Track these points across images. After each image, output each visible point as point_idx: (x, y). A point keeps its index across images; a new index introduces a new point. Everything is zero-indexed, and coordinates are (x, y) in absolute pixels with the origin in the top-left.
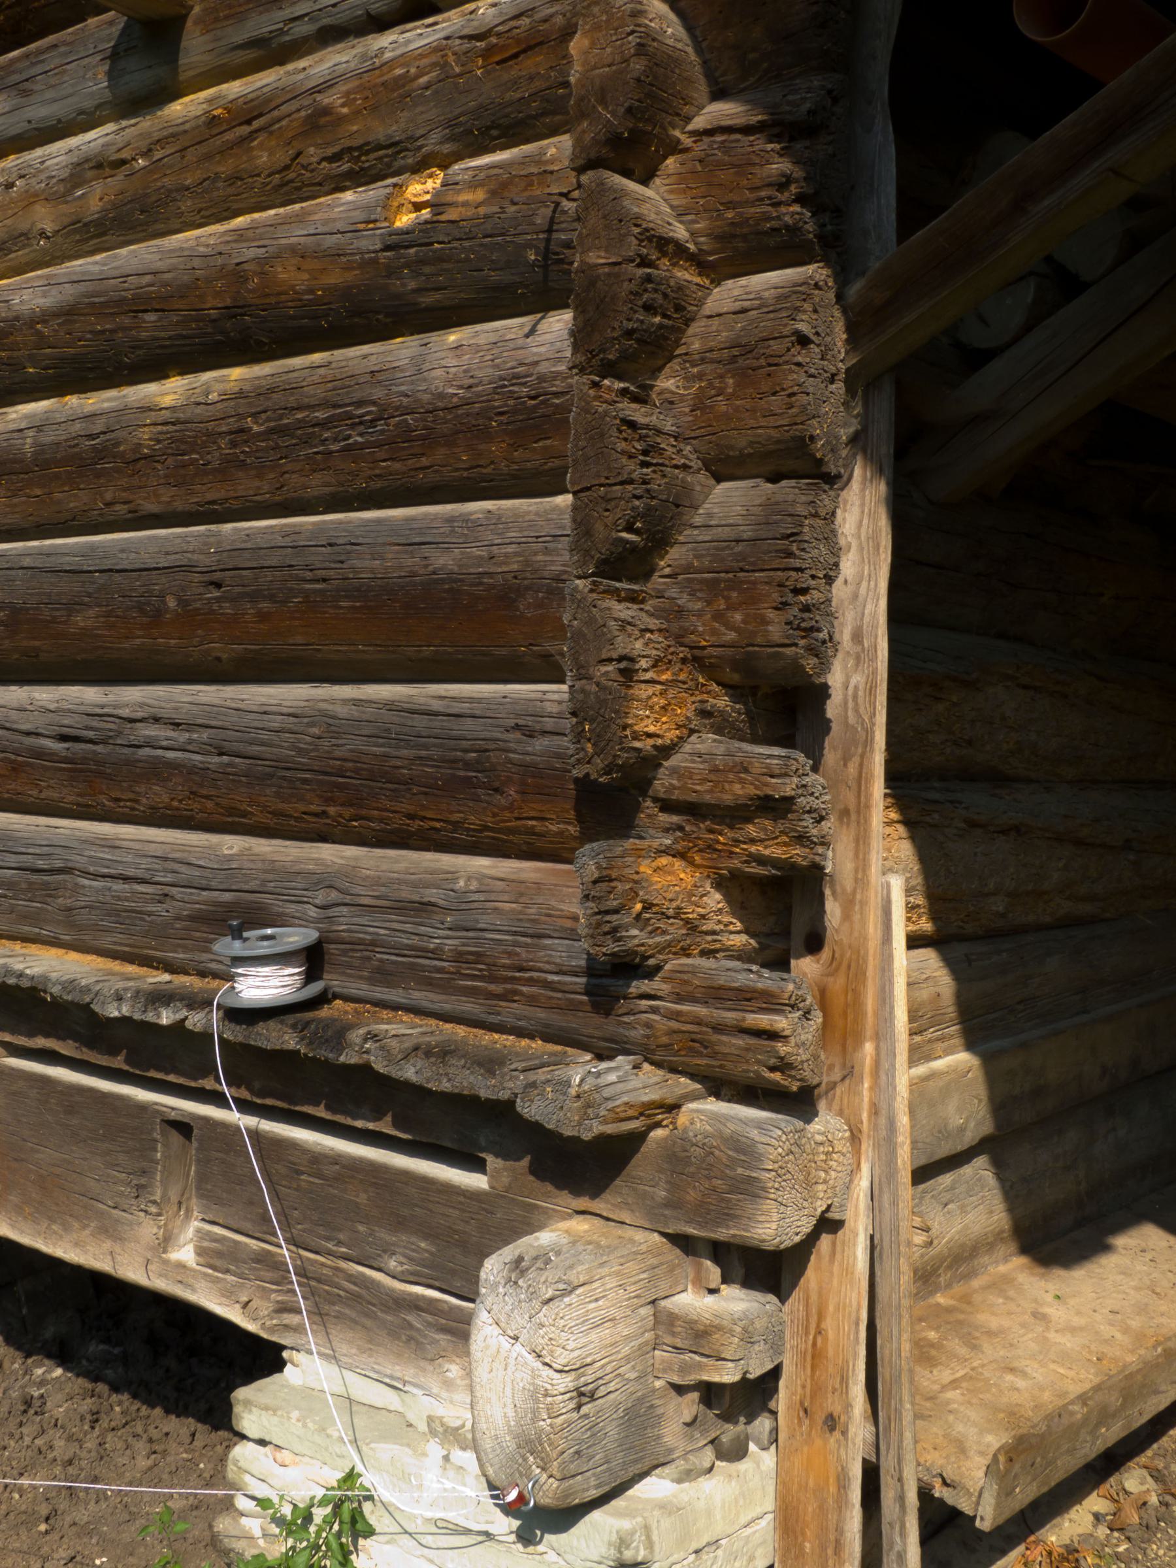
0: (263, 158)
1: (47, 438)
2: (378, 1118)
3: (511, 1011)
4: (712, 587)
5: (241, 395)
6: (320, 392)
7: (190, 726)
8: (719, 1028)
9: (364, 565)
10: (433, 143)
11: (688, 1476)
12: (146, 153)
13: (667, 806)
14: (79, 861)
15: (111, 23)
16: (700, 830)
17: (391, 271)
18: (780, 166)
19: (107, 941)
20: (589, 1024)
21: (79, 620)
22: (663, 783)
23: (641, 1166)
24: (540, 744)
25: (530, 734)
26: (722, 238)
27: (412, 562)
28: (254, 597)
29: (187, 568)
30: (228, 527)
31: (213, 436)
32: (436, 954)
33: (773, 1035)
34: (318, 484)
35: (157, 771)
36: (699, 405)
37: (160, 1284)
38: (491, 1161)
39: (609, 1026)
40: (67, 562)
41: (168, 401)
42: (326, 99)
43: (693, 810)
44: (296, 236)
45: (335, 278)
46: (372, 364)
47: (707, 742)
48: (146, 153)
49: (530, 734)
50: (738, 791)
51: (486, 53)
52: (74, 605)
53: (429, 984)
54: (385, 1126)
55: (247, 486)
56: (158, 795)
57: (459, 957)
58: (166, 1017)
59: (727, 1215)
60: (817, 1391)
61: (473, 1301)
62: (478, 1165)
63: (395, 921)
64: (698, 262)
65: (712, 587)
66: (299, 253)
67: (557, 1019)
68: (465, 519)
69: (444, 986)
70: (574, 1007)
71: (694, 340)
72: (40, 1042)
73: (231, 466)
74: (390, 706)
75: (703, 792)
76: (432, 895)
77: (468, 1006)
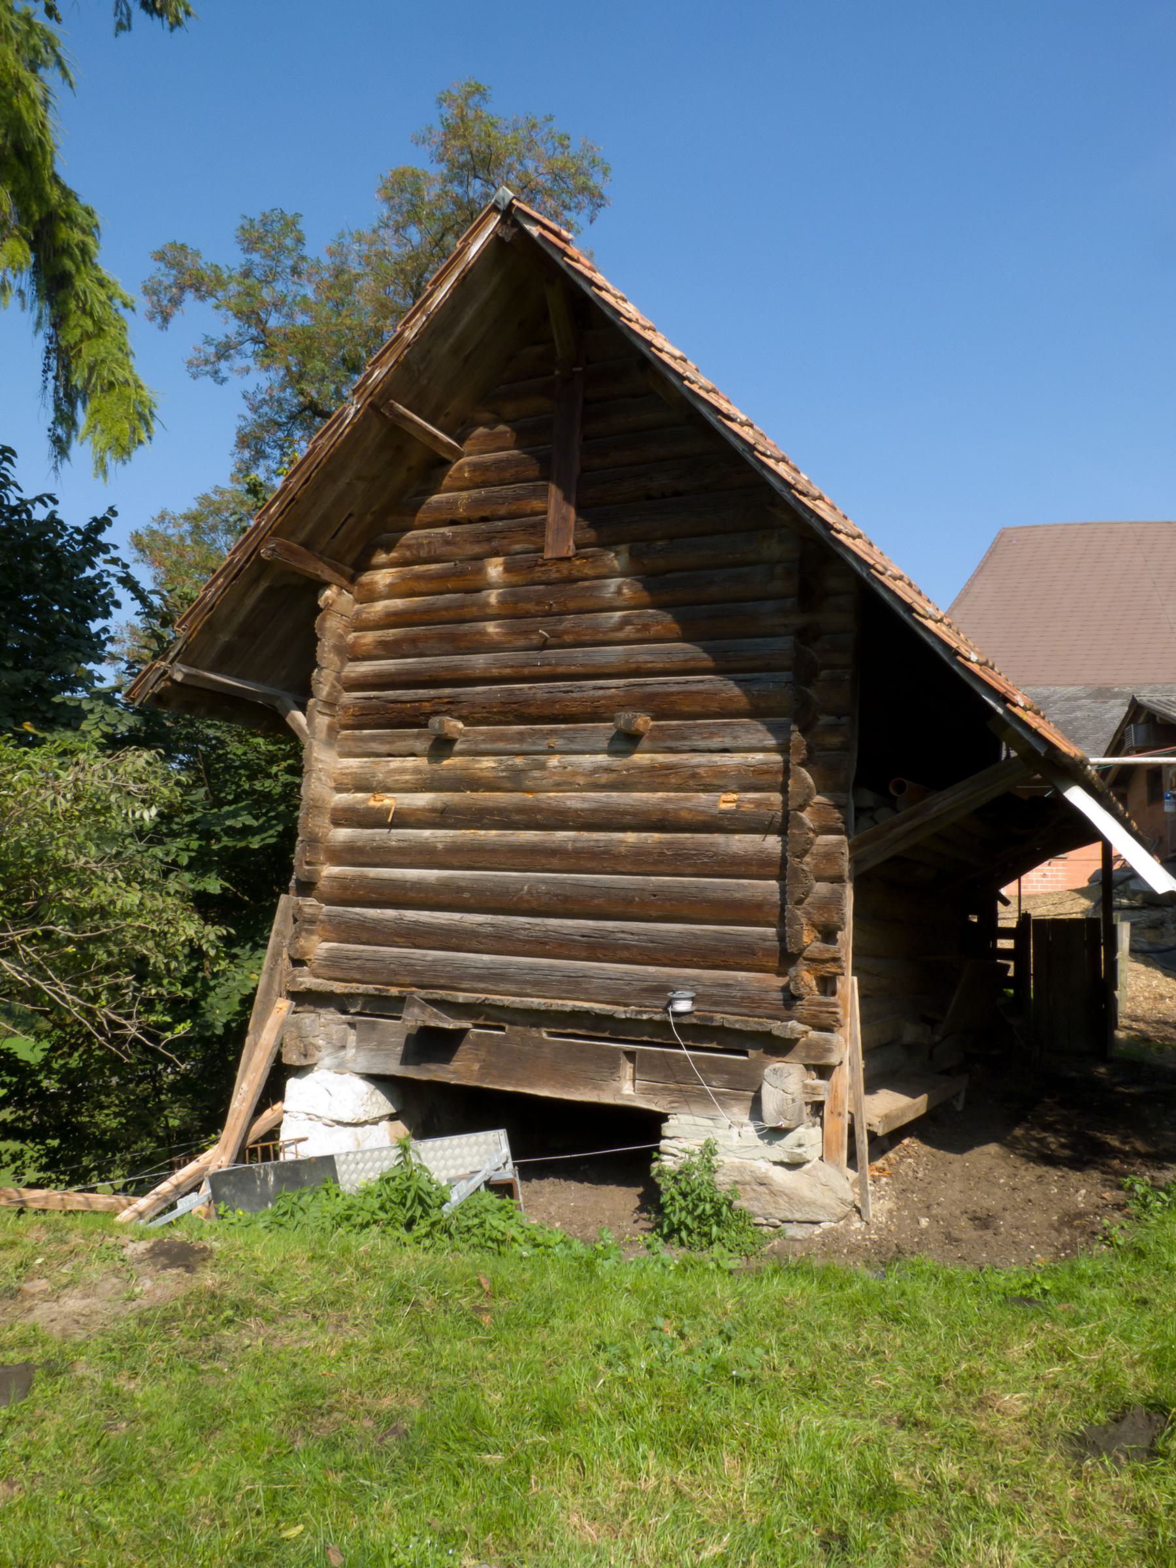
0: (674, 781)
1: (578, 845)
2: (712, 1042)
3: (758, 1011)
4: (819, 908)
5: (661, 843)
6: (692, 846)
7: (638, 935)
8: (821, 1012)
9: (711, 895)
10: (733, 787)
11: (808, 1127)
12: (627, 770)
13: (806, 959)
14: (590, 974)
15: (610, 728)
16: (814, 965)
17: (721, 819)
18: (838, 815)
19: (601, 998)
20: (785, 1013)
21: (596, 902)
22: (805, 954)
23: (797, 1048)
24: (768, 943)
25: (765, 940)
26: (821, 827)
27: (727, 895)
28: (670, 900)
29: (643, 890)
30: (653, 878)
31: (650, 853)
32: (734, 997)
33: (835, 1013)
34: (689, 870)
35: (627, 947)
36: (816, 865)
37: (619, 1102)
38: (751, 1052)
39: (790, 1013)
40: (588, 883)
41: (630, 840)
42: (698, 770)
43: (813, 960)
44: (688, 805)
45: (701, 818)
46: (711, 840)
47: (818, 944)
48: (627, 770)
49: (765, 940)
50: (827, 956)
51: (754, 771)
52: (593, 897)
53: (733, 1005)
54: (714, 1045)
55: (662, 868)
56: (626, 954)
57: (742, 998)
58: (645, 1017)
59: (822, 1058)
60: (835, 1106)
61: (828, 1029)
62: (745, 1054)
63: (719, 989)
64: (814, 831)
65: (819, 908)
66: (690, 810)
67: (774, 1013)
68: (742, 885)
69: (738, 1005)
70: (779, 1009)
71: (814, 849)
72: (569, 1031)
73: (655, 863)
74: (715, 932)
75: (817, 956)
76: (730, 982)
77: (744, 1011)
